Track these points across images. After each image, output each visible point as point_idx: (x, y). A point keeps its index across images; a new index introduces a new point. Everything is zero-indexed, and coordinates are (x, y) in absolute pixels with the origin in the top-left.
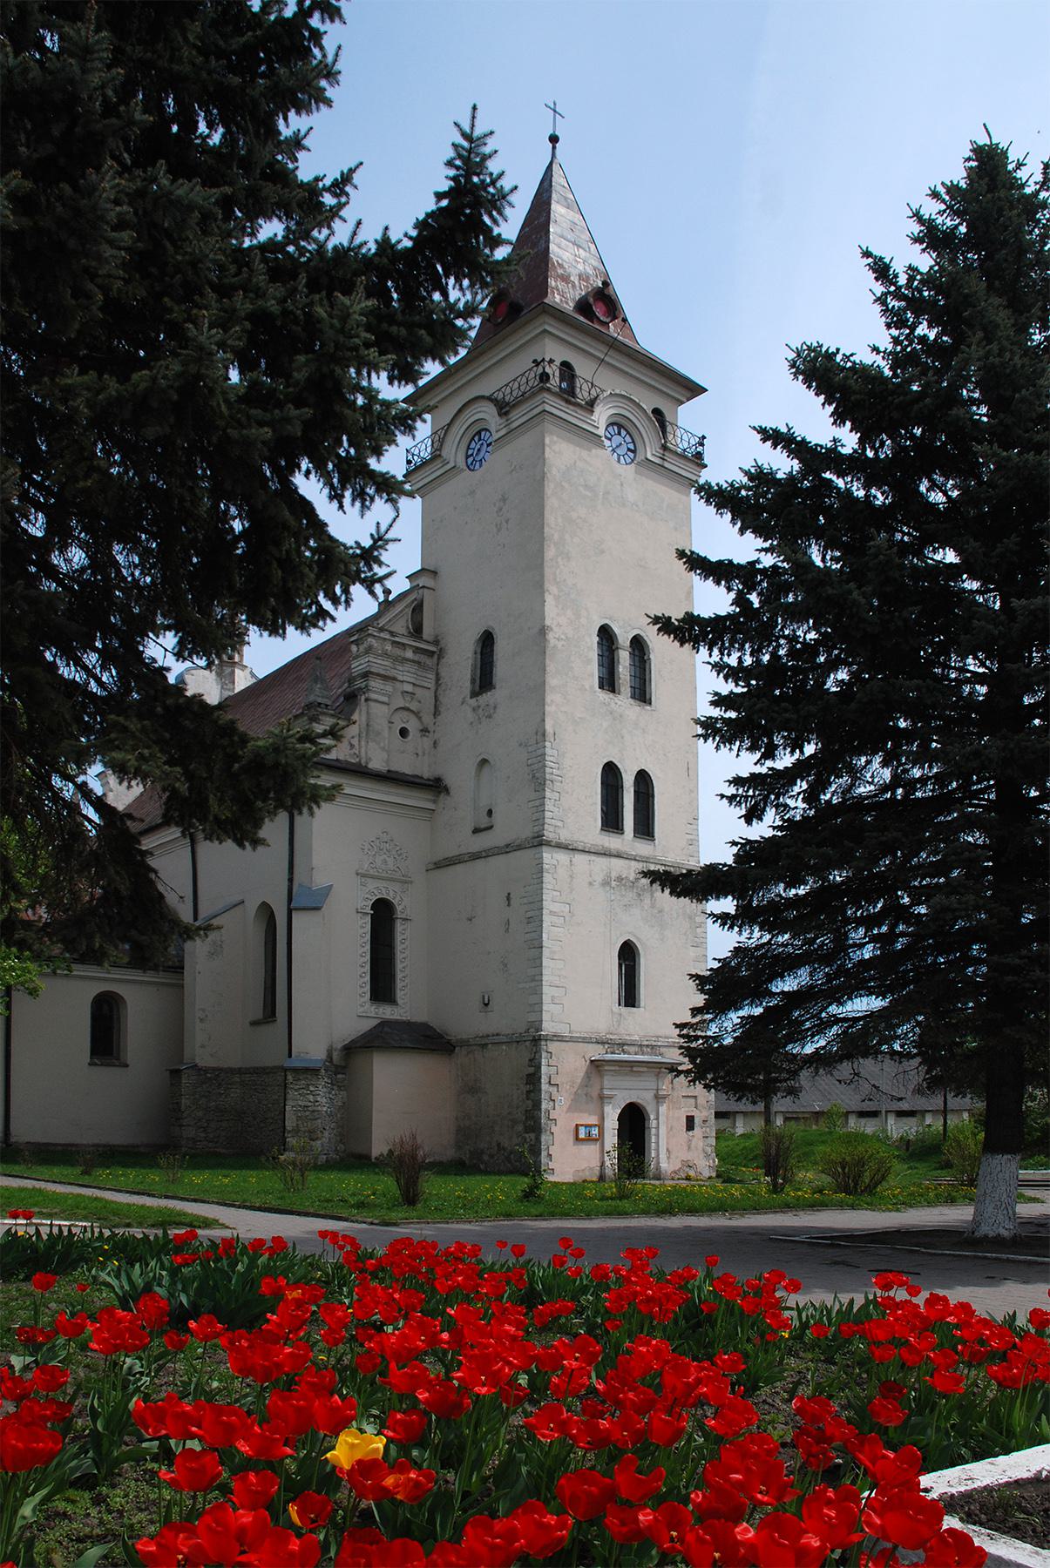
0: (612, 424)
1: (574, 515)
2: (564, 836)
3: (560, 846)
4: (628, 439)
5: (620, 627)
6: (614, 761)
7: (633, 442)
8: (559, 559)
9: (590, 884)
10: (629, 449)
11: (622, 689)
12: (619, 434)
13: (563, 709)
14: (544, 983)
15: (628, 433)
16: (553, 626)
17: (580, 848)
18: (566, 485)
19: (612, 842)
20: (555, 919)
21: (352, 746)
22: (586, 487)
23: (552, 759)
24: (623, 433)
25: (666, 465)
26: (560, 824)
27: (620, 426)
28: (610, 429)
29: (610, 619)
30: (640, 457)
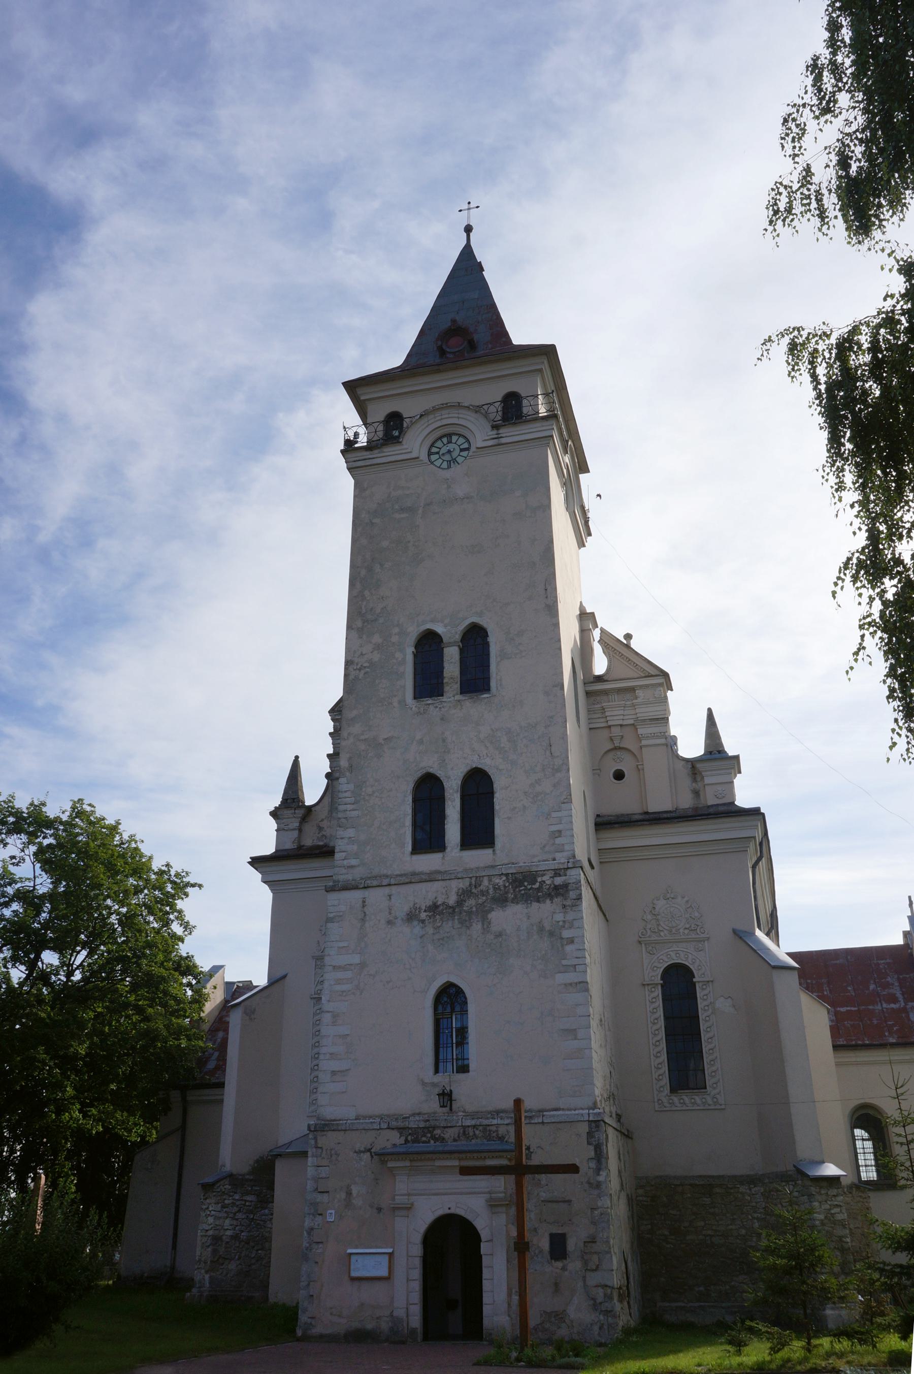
0: (440, 438)
1: (385, 544)
2: (357, 874)
3: (346, 888)
4: (461, 440)
5: (445, 626)
6: (431, 770)
7: (468, 441)
8: (367, 593)
9: (389, 922)
10: (462, 450)
11: (446, 688)
12: (450, 442)
13: (363, 737)
14: (321, 1057)
15: (460, 435)
16: (356, 660)
17: (375, 883)
18: (375, 521)
19: (429, 862)
20: (340, 975)
21: (321, 829)
22: (402, 510)
23: (347, 794)
24: (454, 438)
25: (503, 441)
26: (354, 862)
27: (449, 436)
28: (439, 444)
29: (432, 621)
30: (473, 449)
